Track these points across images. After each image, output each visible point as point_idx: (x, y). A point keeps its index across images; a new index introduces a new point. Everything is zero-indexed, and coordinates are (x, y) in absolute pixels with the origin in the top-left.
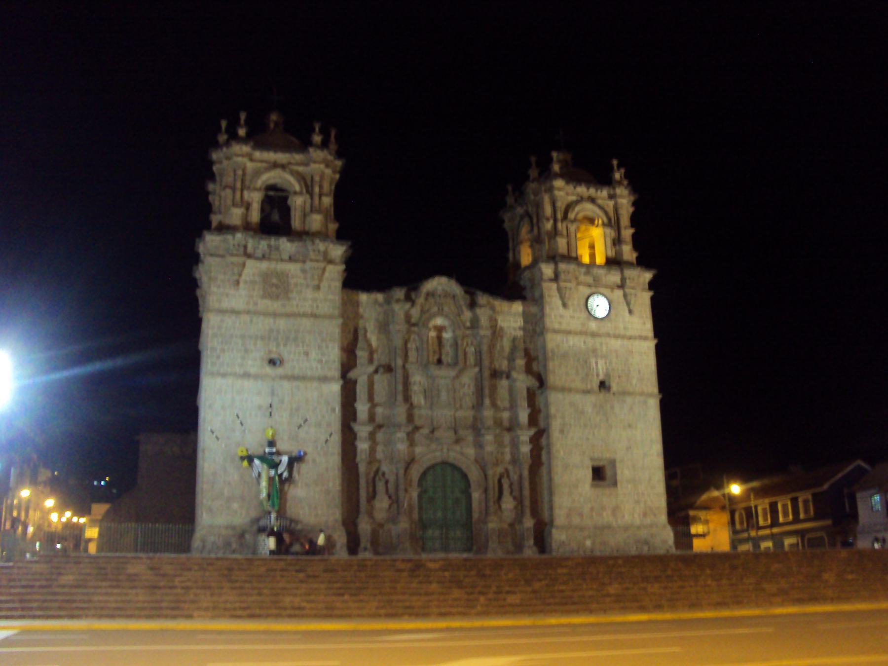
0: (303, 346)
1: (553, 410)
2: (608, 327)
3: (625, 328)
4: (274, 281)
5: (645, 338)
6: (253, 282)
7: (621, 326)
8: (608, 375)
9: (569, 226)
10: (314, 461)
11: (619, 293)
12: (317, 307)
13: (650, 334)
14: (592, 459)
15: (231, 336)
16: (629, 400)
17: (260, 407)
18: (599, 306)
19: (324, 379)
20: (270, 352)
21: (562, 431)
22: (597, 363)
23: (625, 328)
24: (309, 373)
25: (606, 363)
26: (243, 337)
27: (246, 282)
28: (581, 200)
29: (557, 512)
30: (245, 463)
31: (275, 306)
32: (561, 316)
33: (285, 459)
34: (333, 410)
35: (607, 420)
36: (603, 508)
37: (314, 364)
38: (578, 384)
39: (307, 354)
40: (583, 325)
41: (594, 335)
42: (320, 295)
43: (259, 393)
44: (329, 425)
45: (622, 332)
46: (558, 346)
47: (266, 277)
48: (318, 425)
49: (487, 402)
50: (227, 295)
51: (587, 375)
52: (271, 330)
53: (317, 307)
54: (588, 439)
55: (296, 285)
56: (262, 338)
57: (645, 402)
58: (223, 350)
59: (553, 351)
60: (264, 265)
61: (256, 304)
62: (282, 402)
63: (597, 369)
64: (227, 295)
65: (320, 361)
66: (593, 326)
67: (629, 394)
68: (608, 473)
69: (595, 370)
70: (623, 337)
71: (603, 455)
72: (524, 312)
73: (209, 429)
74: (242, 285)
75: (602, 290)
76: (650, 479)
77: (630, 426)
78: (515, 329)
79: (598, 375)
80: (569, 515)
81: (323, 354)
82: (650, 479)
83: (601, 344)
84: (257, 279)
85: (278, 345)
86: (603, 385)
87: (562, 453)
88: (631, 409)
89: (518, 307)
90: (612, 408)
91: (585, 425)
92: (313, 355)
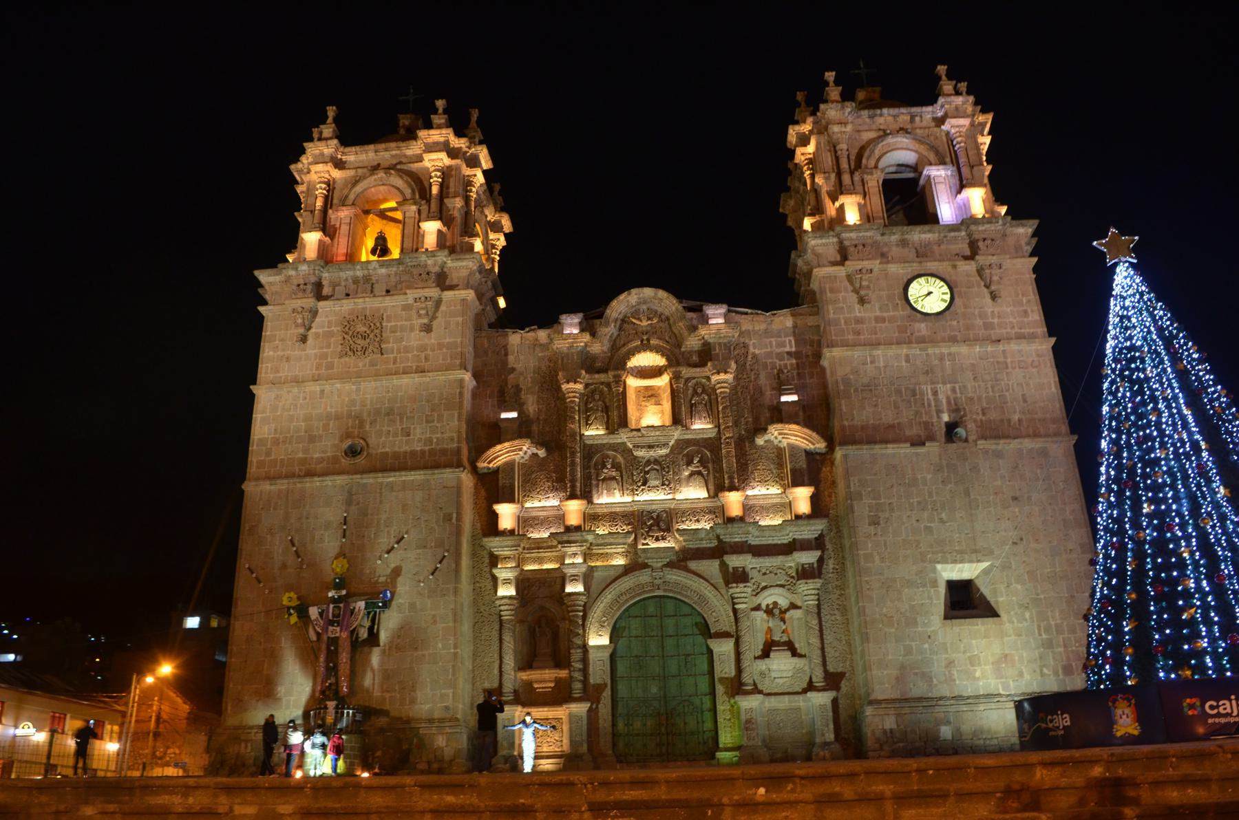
0: (401, 419)
4: (361, 328)
5: (1031, 337)
6: (329, 335)
7: (979, 322)
9: (867, 177)
11: (969, 267)
12: (426, 359)
13: (1042, 329)
23: (988, 326)
27: (317, 335)
28: (885, 134)
31: (362, 363)
32: (859, 321)
35: (967, 493)
40: (902, 330)
42: (432, 339)
47: (348, 325)
51: (917, 413)
53: (426, 359)
54: (929, 530)
55: (394, 330)
59: (846, 381)
60: (347, 306)
61: (330, 366)
63: (937, 400)
66: (922, 328)
69: (933, 404)
72: (795, 326)
73: (247, 566)
74: (310, 341)
75: (932, 266)
77: (1015, 498)
78: (780, 356)
80: (900, 680)
83: (941, 359)
87: (877, 558)
89: (784, 320)
90: (975, 468)
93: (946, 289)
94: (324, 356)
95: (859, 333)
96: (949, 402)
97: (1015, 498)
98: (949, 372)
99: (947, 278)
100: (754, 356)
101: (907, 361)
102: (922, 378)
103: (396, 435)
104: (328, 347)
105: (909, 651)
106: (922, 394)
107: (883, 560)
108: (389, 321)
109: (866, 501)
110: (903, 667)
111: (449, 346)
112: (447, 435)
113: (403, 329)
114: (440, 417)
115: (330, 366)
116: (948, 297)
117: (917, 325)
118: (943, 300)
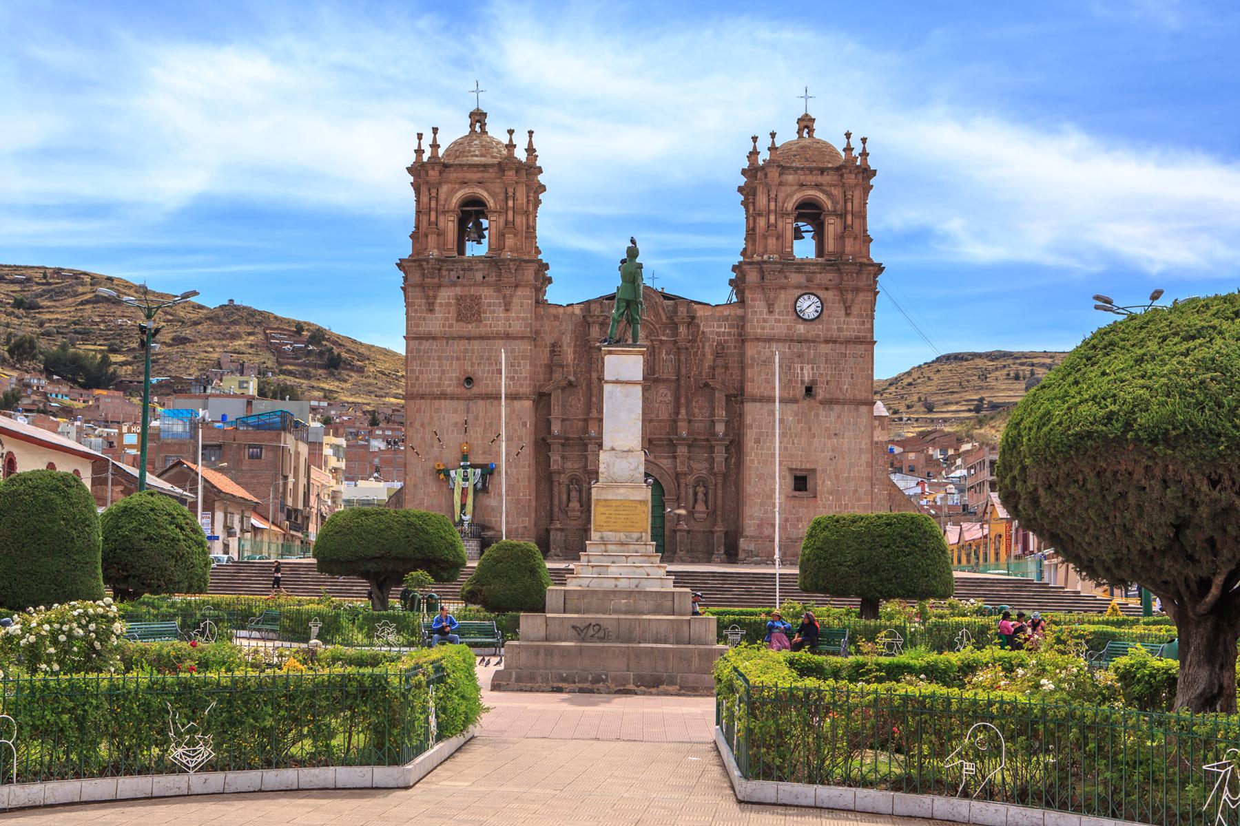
1: (748, 419)
2: (818, 330)
3: (840, 330)
6: (449, 304)
7: (835, 327)
8: (814, 382)
12: (510, 326)
14: (791, 470)
15: (429, 358)
16: (837, 408)
17: (456, 424)
18: (809, 306)
20: (465, 371)
21: (757, 441)
22: (802, 369)
23: (840, 330)
25: (813, 369)
26: (439, 358)
29: (747, 522)
30: (442, 476)
32: (765, 321)
33: (478, 471)
34: (525, 425)
35: (810, 430)
36: (799, 520)
40: (789, 328)
41: (801, 341)
43: (455, 411)
44: (520, 439)
45: (835, 334)
46: (759, 353)
49: (683, 411)
50: (424, 319)
52: (466, 351)
53: (510, 326)
56: (458, 359)
57: (857, 410)
58: (421, 372)
59: (753, 358)
61: (451, 326)
62: (477, 418)
63: (802, 374)
64: (424, 319)
67: (837, 402)
68: (810, 484)
70: (835, 342)
71: (801, 464)
76: (855, 491)
77: (836, 434)
79: (803, 382)
80: (760, 526)
81: (516, 372)
82: (855, 491)
83: (809, 348)
84: (453, 301)
85: (473, 365)
86: (809, 390)
88: (839, 416)
90: (817, 415)
93: (819, 304)
94: (447, 319)
95: (763, 328)
96: (809, 376)
97: (836, 434)
98: (812, 357)
99: (822, 296)
100: (703, 332)
101: (789, 348)
102: (796, 359)
103: (493, 373)
104: (449, 313)
105: (766, 512)
106: (794, 369)
107: (759, 463)
108: (486, 299)
109: (755, 430)
110: (762, 520)
111: (524, 319)
112: (524, 375)
113: (494, 304)
114: (519, 365)
115: (451, 326)
116: (819, 309)
117: (798, 326)
118: (816, 311)
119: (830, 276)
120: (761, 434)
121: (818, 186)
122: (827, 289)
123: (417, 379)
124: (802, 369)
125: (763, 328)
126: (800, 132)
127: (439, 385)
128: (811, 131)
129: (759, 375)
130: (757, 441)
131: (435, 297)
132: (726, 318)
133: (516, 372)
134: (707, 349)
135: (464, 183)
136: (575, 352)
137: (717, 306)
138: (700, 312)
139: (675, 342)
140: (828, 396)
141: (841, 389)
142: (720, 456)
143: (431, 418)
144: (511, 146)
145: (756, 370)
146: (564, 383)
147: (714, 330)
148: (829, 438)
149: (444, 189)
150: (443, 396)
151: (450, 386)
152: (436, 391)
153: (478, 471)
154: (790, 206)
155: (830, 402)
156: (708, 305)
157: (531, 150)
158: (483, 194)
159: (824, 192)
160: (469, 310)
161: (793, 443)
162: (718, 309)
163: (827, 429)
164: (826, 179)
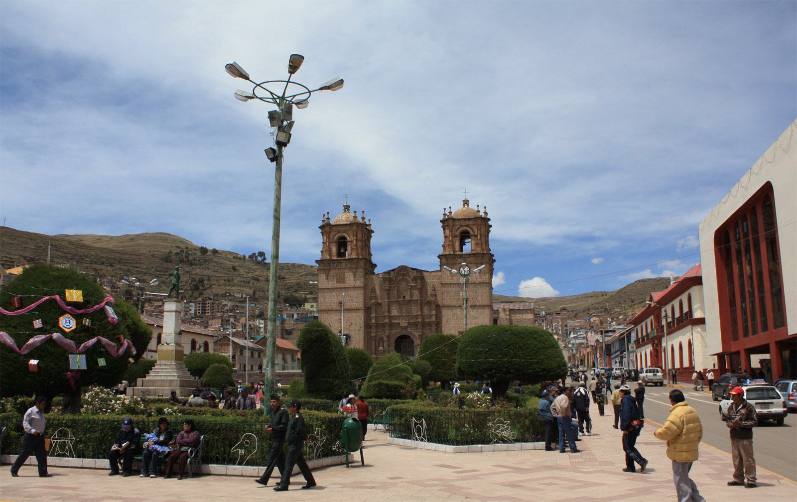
1: (443, 314)
7: (475, 277)
10: (355, 337)
17: (336, 320)
19: (357, 310)
22: (463, 294)
24: (353, 307)
33: (345, 337)
37: (354, 303)
38: (454, 303)
39: (352, 300)
44: (360, 324)
48: (356, 325)
65: (356, 302)
77: (476, 318)
81: (357, 299)
91: (457, 319)
92: (354, 301)
97: (476, 318)
112: (360, 301)
119: (472, 259)
120: (448, 319)
121: (467, 226)
122: (471, 264)
123: (322, 304)
124: (463, 294)
125: (448, 279)
126: (464, 205)
127: (330, 305)
128: (468, 205)
129: (447, 296)
130: (447, 322)
131: (328, 274)
132: (435, 276)
133: (357, 299)
134: (429, 288)
135: (339, 232)
136: (380, 291)
137: (432, 272)
138: (425, 274)
139: (416, 286)
140: (473, 304)
141: (477, 301)
142: (434, 328)
143: (328, 318)
144: (355, 217)
145: (446, 295)
146: (376, 303)
147: (430, 281)
148: (474, 319)
149: (332, 234)
150: (332, 310)
151: (335, 307)
152: (329, 308)
153: (345, 337)
154: (457, 233)
155: (473, 307)
156: (428, 271)
157: (363, 218)
158: (346, 235)
159: (471, 228)
160: (341, 280)
161: (460, 322)
162: (432, 273)
163: (472, 316)
164: (470, 222)
